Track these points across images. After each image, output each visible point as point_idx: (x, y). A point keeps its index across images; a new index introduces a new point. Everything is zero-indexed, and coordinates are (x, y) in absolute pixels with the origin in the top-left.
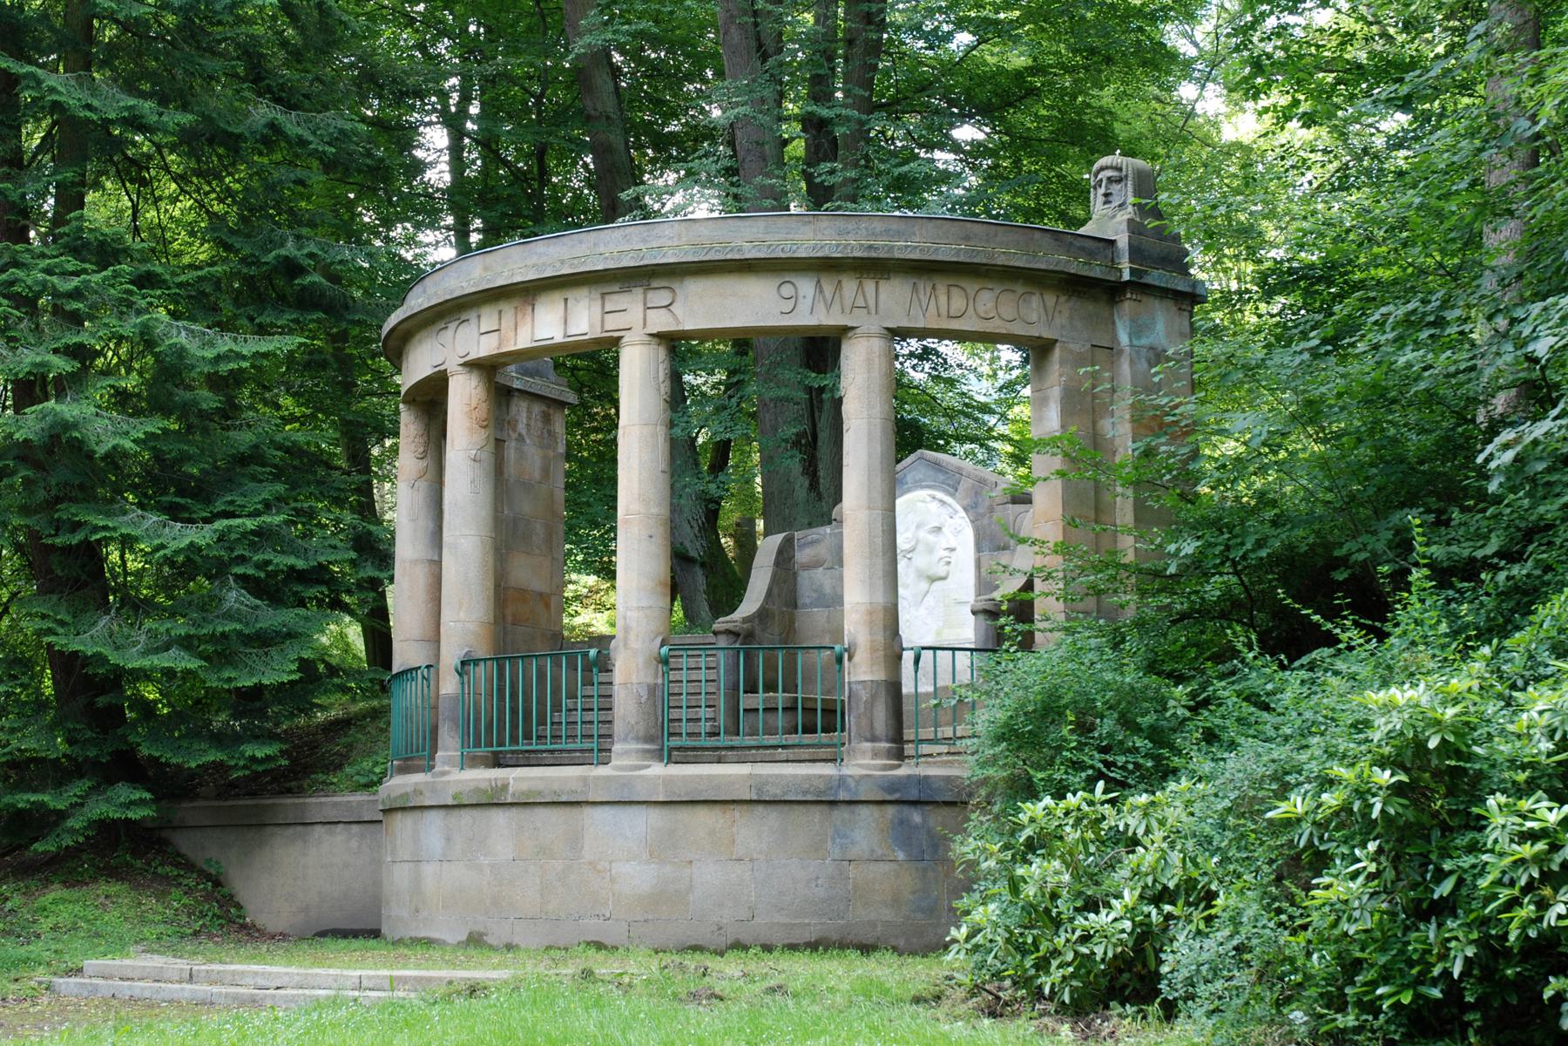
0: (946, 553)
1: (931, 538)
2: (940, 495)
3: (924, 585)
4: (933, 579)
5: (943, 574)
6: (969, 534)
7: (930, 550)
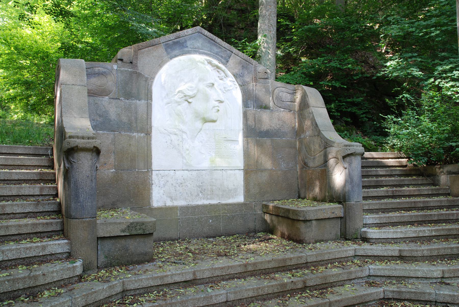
0: (217, 104)
1: (208, 90)
2: (215, 62)
3: (199, 124)
4: (205, 121)
5: (215, 119)
6: (237, 95)
7: (207, 98)
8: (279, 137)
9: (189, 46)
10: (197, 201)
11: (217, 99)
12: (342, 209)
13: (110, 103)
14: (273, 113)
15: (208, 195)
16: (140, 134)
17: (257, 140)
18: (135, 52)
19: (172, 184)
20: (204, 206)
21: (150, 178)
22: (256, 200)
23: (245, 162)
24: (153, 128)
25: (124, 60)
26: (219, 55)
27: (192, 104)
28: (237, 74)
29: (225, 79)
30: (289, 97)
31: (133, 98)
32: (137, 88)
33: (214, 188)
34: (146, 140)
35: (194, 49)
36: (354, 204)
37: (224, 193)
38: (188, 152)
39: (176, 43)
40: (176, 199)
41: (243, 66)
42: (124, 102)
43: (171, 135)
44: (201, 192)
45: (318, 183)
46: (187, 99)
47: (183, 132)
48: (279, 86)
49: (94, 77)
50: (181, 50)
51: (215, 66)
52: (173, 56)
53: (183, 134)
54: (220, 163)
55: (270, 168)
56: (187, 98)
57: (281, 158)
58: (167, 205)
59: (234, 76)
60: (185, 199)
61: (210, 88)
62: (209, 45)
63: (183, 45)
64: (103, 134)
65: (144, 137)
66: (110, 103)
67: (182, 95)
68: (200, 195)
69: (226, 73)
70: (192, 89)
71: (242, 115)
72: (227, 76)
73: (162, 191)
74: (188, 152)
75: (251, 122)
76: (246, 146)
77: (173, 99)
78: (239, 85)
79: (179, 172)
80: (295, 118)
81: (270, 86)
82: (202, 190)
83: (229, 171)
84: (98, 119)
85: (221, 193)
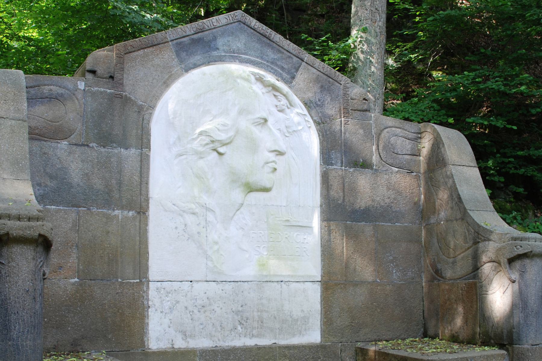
0: (272, 157)
1: (257, 131)
2: (270, 78)
3: (237, 195)
4: (251, 188)
5: (268, 185)
7: (253, 146)
8: (390, 221)
9: (221, 48)
10: (232, 340)
11: (273, 149)
12: (507, 357)
13: (70, 153)
14: (377, 176)
15: (254, 328)
16: (126, 212)
17: (346, 227)
18: (120, 57)
19: (186, 307)
20: (246, 350)
21: (144, 295)
22: (344, 340)
23: (323, 267)
24: (150, 201)
25: (99, 72)
26: (277, 65)
27: (224, 156)
28: (311, 102)
29: (288, 111)
30: (408, 145)
31: (115, 145)
32: (122, 126)
33: (265, 315)
34: (137, 224)
35: (231, 52)
36: (528, 350)
37: (284, 326)
38: (216, 247)
39: (196, 42)
40: (192, 336)
41: (322, 87)
42: (96, 151)
43: (185, 215)
44: (241, 324)
45: (460, 309)
46: (217, 147)
47: (208, 209)
48: (390, 124)
49: (42, 103)
50: (206, 55)
51: (269, 86)
52: (191, 66)
53: (209, 214)
54: (278, 268)
55: (370, 279)
56: (216, 145)
57: (392, 261)
58: (176, 346)
59: (305, 104)
60: (211, 336)
61: (259, 127)
62: (258, 46)
63: (210, 46)
64: (57, 211)
65: (134, 218)
66: (70, 153)
67: (208, 140)
68: (239, 328)
69: (290, 98)
70: (226, 128)
71: (318, 178)
72: (291, 105)
73: (166, 321)
74: (216, 247)
75: (336, 192)
76: (326, 237)
77: (189, 146)
78: (315, 121)
79: (200, 283)
80: (419, 186)
81: (374, 125)
82: (242, 321)
83: (294, 284)
84: (49, 183)
85: (277, 326)
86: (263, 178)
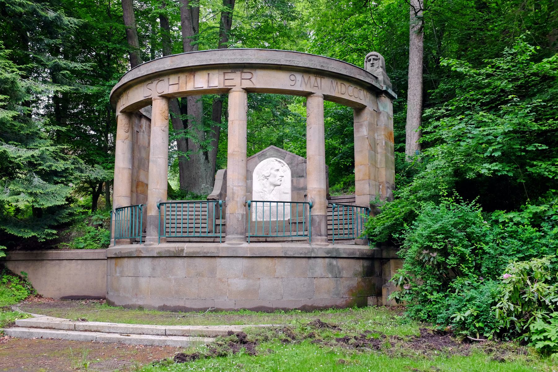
1: (276, 173)
2: (279, 160)
3: (272, 187)
7: (275, 176)
46: (267, 177)
86: (279, 183)
